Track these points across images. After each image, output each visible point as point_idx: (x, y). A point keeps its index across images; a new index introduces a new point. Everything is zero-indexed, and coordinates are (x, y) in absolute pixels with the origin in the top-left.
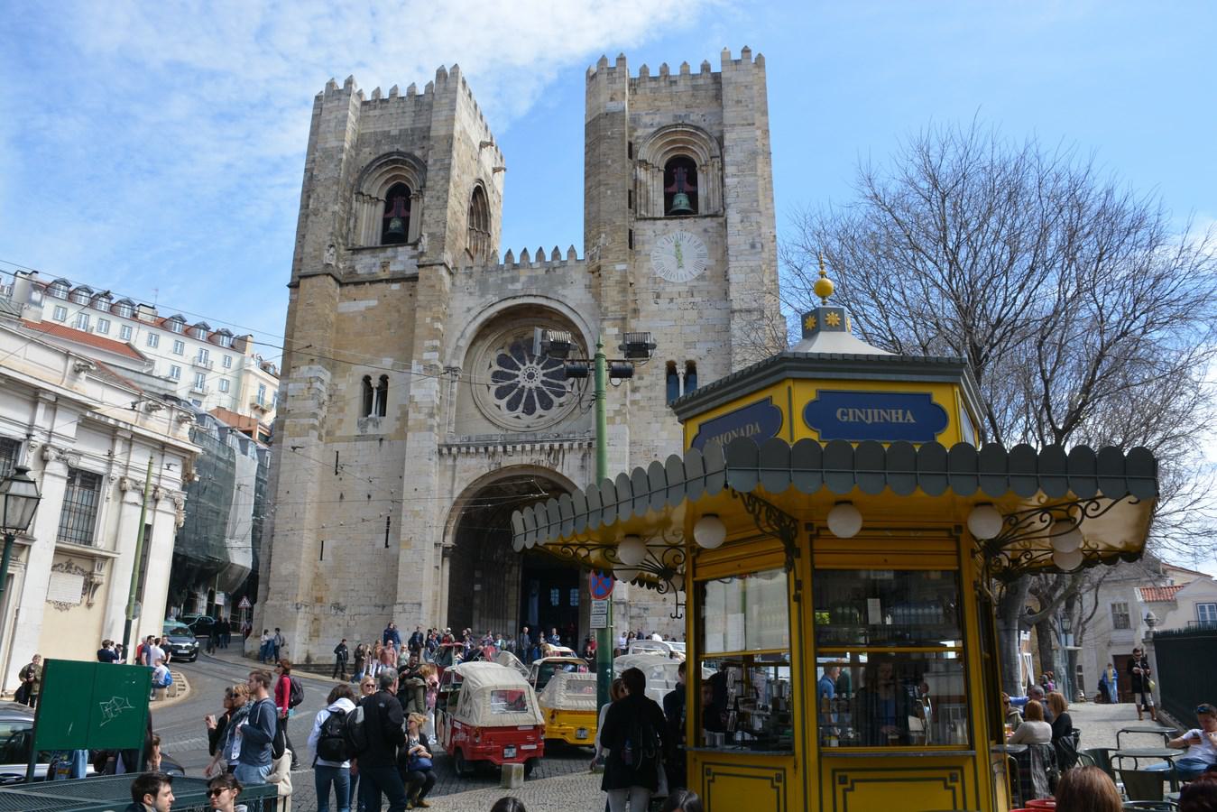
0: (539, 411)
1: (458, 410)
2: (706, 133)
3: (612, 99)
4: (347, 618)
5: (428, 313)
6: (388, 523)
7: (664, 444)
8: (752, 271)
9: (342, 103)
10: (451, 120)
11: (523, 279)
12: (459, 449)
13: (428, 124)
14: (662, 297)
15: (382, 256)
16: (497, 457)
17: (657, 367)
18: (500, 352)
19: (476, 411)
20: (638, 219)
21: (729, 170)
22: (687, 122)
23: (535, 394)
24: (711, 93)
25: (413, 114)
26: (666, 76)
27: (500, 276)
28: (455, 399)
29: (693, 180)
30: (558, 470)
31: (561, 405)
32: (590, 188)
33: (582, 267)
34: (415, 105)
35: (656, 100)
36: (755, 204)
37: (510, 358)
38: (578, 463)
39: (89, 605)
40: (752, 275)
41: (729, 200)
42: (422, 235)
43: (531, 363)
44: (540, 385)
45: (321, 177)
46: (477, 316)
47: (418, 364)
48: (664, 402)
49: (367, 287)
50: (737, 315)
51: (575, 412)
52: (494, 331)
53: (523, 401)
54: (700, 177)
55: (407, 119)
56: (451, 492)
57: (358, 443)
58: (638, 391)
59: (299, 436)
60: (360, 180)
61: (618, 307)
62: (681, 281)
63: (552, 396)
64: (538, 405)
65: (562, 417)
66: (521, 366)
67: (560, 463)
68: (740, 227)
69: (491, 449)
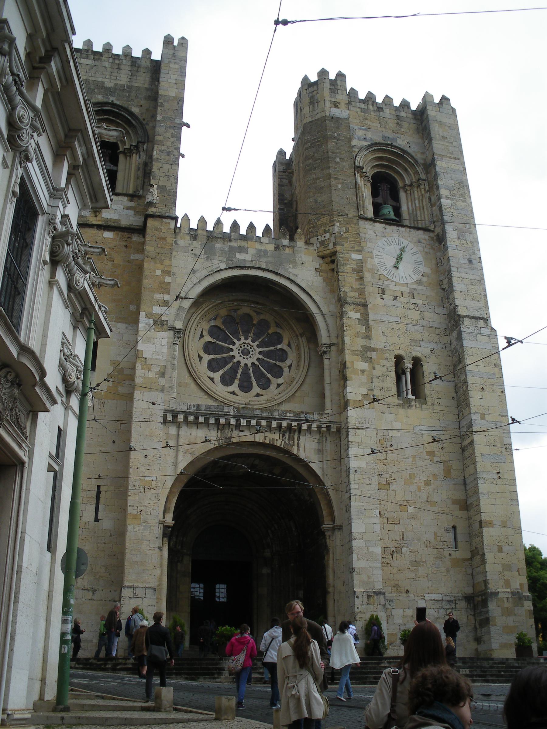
0: (256, 389)
3: (336, 107)
5: (158, 265)
6: (99, 492)
8: (472, 284)
10: (181, 84)
11: (251, 251)
12: (186, 418)
14: (386, 293)
17: (386, 359)
18: (213, 323)
19: (189, 380)
21: (443, 192)
22: (394, 144)
24: (414, 126)
31: (279, 385)
40: (471, 287)
41: (446, 218)
43: (246, 339)
44: (257, 363)
46: (202, 280)
51: (296, 395)
53: (239, 376)
54: (402, 195)
56: (176, 465)
61: (357, 294)
62: (402, 282)
63: (269, 376)
64: (254, 383)
65: (284, 398)
66: (235, 341)
68: (457, 242)
69: (223, 421)
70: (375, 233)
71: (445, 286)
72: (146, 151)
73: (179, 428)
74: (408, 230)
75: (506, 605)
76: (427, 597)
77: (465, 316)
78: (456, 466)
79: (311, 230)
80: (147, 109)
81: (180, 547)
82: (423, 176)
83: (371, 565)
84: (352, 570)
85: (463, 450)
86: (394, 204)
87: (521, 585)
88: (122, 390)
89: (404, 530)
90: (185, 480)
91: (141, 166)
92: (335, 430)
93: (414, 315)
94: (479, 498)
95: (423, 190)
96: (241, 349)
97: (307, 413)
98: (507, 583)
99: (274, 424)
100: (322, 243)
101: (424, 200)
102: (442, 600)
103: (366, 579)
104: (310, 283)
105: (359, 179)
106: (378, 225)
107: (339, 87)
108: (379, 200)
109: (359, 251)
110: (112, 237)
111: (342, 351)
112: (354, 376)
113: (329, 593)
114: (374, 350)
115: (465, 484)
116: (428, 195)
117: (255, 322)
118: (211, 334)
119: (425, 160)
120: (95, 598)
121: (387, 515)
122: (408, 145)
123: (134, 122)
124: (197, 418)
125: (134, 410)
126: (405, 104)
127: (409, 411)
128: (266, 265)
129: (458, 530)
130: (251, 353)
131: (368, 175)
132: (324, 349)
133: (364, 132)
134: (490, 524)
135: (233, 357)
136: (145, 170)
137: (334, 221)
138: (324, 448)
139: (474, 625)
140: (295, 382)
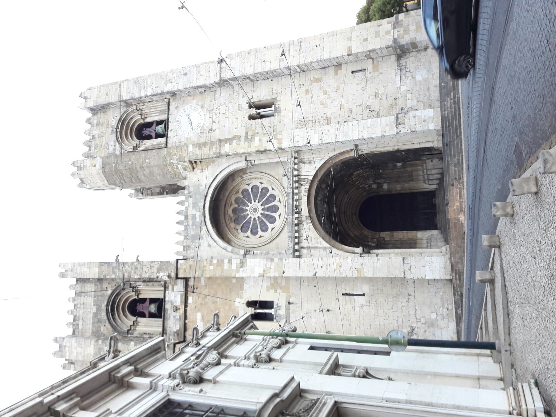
0: (276, 203)
3: (95, 166)
4: (419, 325)
5: (207, 268)
6: (346, 294)
8: (199, 73)
9: (68, 345)
10: (90, 265)
11: (194, 212)
12: (297, 244)
13: (93, 285)
18: (239, 231)
19: (274, 242)
21: (143, 94)
22: (115, 127)
23: (266, 206)
24: (102, 114)
27: (191, 227)
29: (150, 125)
30: (311, 178)
31: (273, 189)
32: (144, 175)
35: (101, 145)
36: (163, 77)
37: (243, 225)
38: (307, 165)
40: (201, 72)
41: (159, 92)
42: (158, 277)
43: (247, 210)
44: (261, 203)
46: (214, 240)
47: (238, 272)
48: (272, 118)
49: (189, 322)
51: (277, 178)
52: (226, 234)
53: (269, 213)
54: (148, 120)
55: (88, 301)
60: (119, 333)
61: (213, 146)
63: (268, 195)
64: (273, 204)
65: (280, 185)
66: (249, 217)
68: (174, 83)
69: (296, 222)
71: (203, 90)
72: (135, 282)
73: (302, 248)
74: (170, 116)
75: (402, 32)
76: (398, 85)
77: (220, 76)
78: (313, 75)
79: (177, 177)
80: (109, 284)
81: (375, 240)
82: (135, 107)
84: (383, 137)
85: (304, 71)
86: (154, 125)
87: (388, 23)
88: (283, 284)
89: (356, 105)
90: (334, 242)
91: (146, 284)
92: (297, 154)
93: (223, 109)
94: (333, 58)
95: (143, 107)
96: (253, 213)
98: (387, 33)
99: (296, 191)
100: (185, 169)
101: (150, 106)
102: (400, 75)
103: (388, 127)
105: (141, 148)
106: (169, 135)
108: (153, 135)
109: (186, 145)
111: (250, 154)
112: (264, 145)
113: (398, 149)
114: (247, 134)
115: (325, 68)
116: (146, 104)
117: (237, 206)
119: (123, 107)
120: (413, 294)
121: (346, 117)
122: (115, 117)
123: (117, 291)
124: (296, 237)
125: (295, 276)
126: (88, 121)
127: (282, 108)
129: (354, 69)
130: (255, 207)
131: (138, 143)
132: (249, 164)
133: (110, 147)
134: (349, 49)
135: (258, 217)
136: (148, 281)
137: (170, 163)
138: (308, 160)
139: (416, 53)
140: (270, 180)
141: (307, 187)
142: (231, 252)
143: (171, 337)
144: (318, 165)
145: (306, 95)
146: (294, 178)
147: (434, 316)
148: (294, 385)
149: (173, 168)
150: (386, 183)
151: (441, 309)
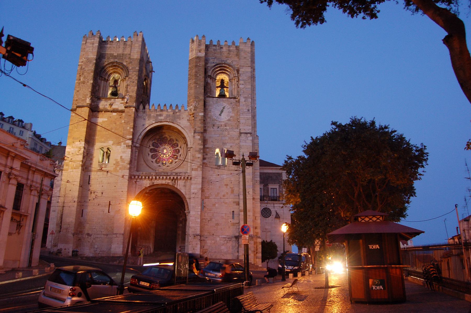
1: (138, 162)
2: (233, 67)
3: (200, 52)
7: (214, 179)
9: (95, 41)
11: (164, 115)
13: (129, 53)
14: (215, 126)
15: (109, 102)
16: (153, 180)
18: (154, 141)
20: (207, 97)
21: (241, 82)
22: (226, 63)
24: (235, 53)
25: (123, 48)
26: (219, 45)
27: (156, 114)
28: (136, 158)
31: (176, 162)
32: (191, 84)
33: (186, 113)
34: (124, 45)
35: (215, 53)
38: (183, 184)
39: (19, 233)
45: (86, 69)
49: (103, 114)
50: (243, 135)
51: (181, 165)
57: (98, 173)
58: (206, 159)
59: (75, 169)
67: (176, 184)
68: (244, 103)
69: (151, 177)
70: (213, 102)
80: (129, 63)
83: (196, 225)
97: (180, 173)
99: (168, 177)
104: (185, 126)
107: (202, 43)
110: (115, 115)
114: (208, 148)
118: (153, 145)
119: (238, 68)
128: (169, 120)
141: (171, 184)
142: (138, 138)
143: (95, 103)
144: (183, 191)
145: (225, 184)
146: (176, 177)
147: (96, 246)
148: (4, 210)
149: (191, 102)
150: (183, 225)
151: (99, 250)
